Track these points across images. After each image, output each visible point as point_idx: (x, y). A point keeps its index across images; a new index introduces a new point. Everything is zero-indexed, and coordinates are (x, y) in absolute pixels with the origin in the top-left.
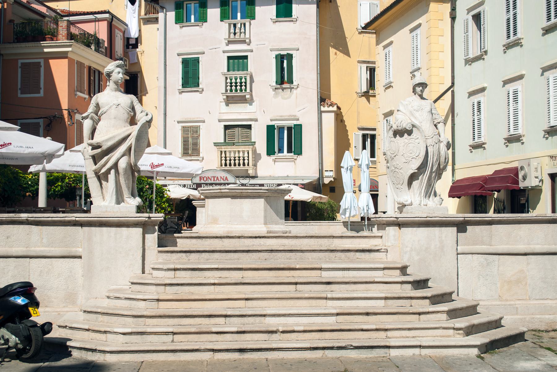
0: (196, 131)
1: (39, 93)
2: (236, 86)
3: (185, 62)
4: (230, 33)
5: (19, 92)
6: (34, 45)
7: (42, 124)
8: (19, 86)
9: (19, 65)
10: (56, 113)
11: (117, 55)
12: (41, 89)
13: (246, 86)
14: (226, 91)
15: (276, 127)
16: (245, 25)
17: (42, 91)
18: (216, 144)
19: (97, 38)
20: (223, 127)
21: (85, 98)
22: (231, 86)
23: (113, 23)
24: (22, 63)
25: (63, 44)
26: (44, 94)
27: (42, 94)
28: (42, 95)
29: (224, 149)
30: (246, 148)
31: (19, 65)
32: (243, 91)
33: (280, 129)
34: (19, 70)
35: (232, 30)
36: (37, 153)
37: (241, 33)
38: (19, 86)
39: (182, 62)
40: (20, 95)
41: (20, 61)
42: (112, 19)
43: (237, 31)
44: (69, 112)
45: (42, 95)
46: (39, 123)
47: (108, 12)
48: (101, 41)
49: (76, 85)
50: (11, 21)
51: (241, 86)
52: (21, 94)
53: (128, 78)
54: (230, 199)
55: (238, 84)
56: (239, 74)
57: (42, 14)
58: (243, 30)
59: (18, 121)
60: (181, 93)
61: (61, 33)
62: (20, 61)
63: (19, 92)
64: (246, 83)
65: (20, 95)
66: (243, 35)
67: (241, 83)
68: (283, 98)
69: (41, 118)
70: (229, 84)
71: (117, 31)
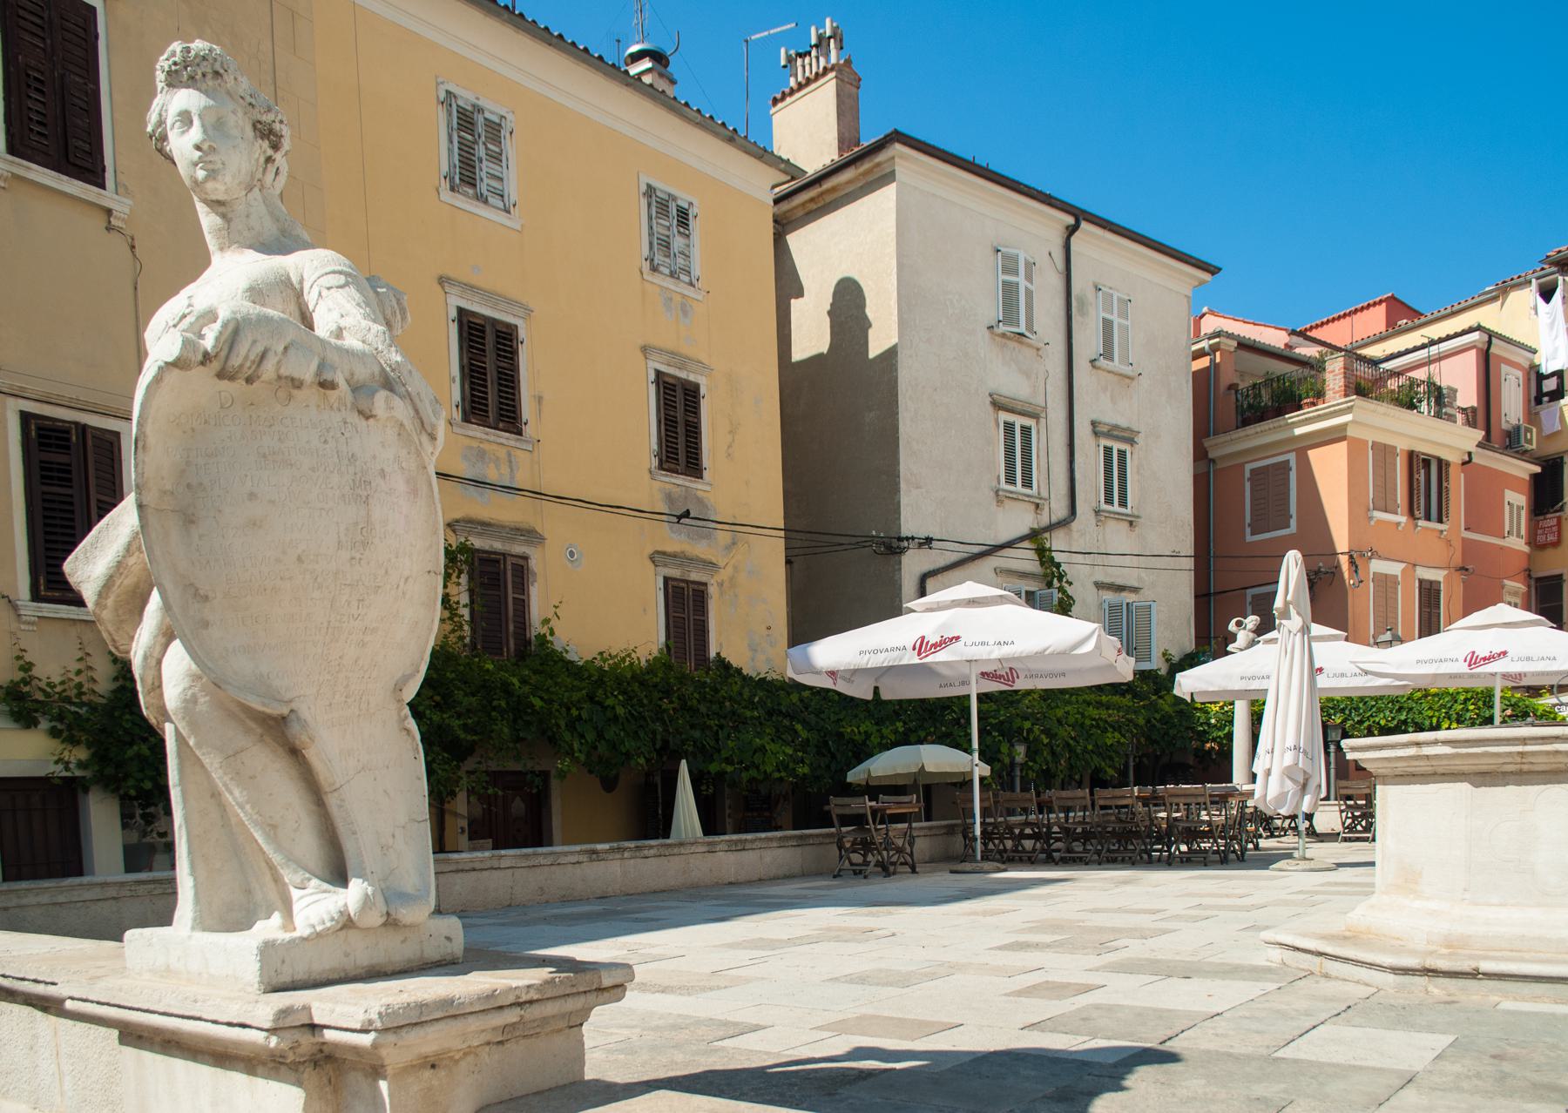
1: (1288, 526)
5: (1248, 530)
10: (1321, 564)
11: (1507, 422)
12: (1291, 517)
19: (1434, 384)
21: (1398, 524)
23: (1493, 350)
25: (1332, 409)
34: (1248, 486)
36: (1024, 655)
40: (1249, 538)
41: (1248, 467)
42: (1490, 342)
44: (1351, 557)
47: (1479, 328)
48: (1445, 391)
49: (1371, 496)
50: (1232, 387)
52: (1252, 534)
53: (1538, 469)
54: (1464, 788)
57: (1257, 345)
59: (1248, 591)
61: (1331, 386)
65: (1249, 538)
71: (1504, 368)
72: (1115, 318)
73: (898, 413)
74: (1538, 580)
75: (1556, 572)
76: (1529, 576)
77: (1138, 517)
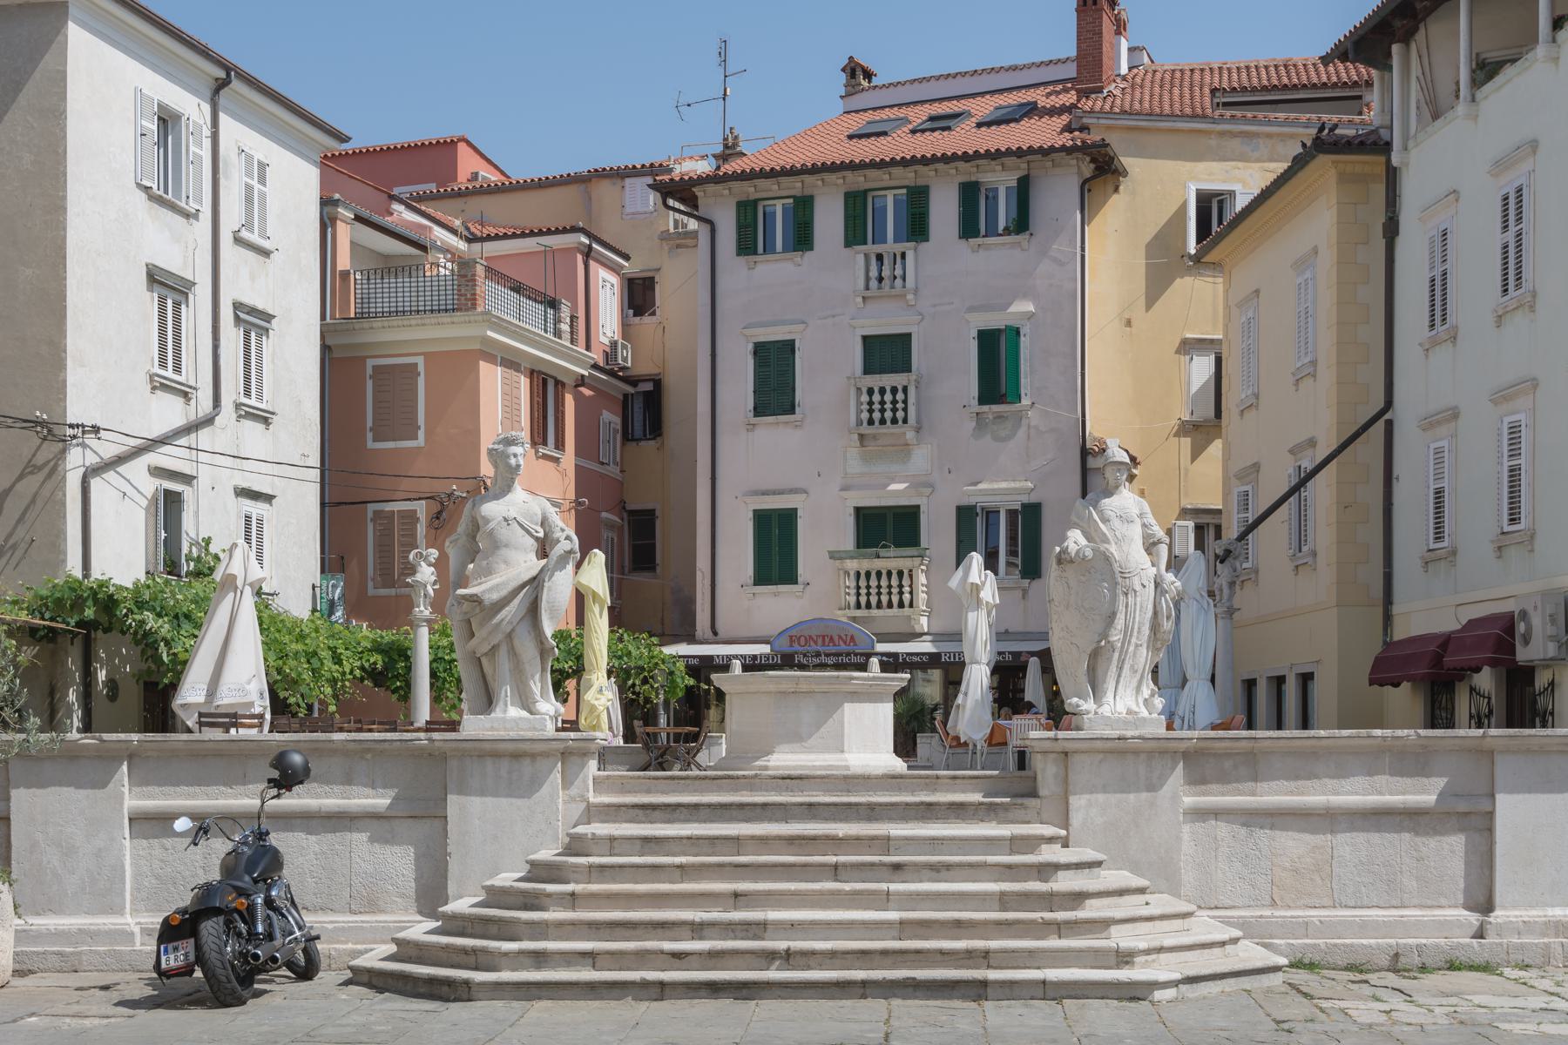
0: (787, 519)
2: (882, 411)
3: (761, 350)
4: (868, 279)
5: (370, 435)
6: (400, 323)
7: (422, 515)
8: (369, 423)
9: (369, 371)
12: (419, 428)
13: (905, 410)
14: (859, 423)
15: (979, 510)
16: (903, 256)
17: (421, 434)
18: (834, 555)
20: (852, 511)
22: (871, 411)
24: (374, 367)
26: (427, 440)
27: (421, 440)
28: (422, 444)
29: (852, 565)
30: (904, 564)
31: (369, 371)
32: (900, 422)
33: (990, 515)
34: (370, 384)
35: (874, 273)
37: (895, 277)
38: (369, 423)
39: (755, 353)
40: (371, 444)
43: (886, 273)
45: (422, 444)
46: (415, 511)
51: (894, 410)
55: (888, 406)
56: (888, 380)
58: (898, 272)
60: (752, 427)
62: (370, 363)
63: (370, 435)
64: (905, 402)
65: (371, 444)
66: (898, 282)
67: (894, 402)
68: (996, 439)
69: (420, 499)
70: (865, 407)
72: (257, 186)
73: (65, 279)
74: (632, 513)
75: (649, 506)
76: (624, 508)
77: (273, 413)
